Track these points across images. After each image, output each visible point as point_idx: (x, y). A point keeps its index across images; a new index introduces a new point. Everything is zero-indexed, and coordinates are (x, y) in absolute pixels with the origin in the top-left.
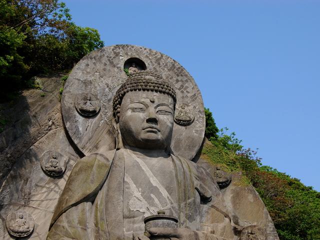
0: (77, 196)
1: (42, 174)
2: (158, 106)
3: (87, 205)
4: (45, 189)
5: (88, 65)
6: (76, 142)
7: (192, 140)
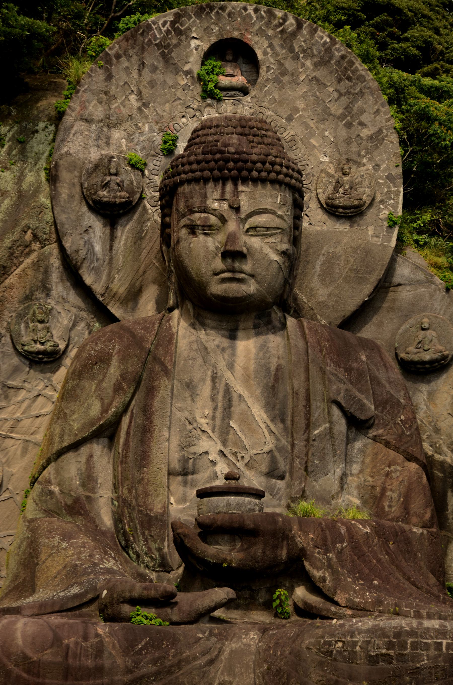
0: (77, 424)
1: (16, 360)
3: (97, 449)
4: (22, 394)
5: (109, 77)
6: (88, 279)
7: (366, 252)
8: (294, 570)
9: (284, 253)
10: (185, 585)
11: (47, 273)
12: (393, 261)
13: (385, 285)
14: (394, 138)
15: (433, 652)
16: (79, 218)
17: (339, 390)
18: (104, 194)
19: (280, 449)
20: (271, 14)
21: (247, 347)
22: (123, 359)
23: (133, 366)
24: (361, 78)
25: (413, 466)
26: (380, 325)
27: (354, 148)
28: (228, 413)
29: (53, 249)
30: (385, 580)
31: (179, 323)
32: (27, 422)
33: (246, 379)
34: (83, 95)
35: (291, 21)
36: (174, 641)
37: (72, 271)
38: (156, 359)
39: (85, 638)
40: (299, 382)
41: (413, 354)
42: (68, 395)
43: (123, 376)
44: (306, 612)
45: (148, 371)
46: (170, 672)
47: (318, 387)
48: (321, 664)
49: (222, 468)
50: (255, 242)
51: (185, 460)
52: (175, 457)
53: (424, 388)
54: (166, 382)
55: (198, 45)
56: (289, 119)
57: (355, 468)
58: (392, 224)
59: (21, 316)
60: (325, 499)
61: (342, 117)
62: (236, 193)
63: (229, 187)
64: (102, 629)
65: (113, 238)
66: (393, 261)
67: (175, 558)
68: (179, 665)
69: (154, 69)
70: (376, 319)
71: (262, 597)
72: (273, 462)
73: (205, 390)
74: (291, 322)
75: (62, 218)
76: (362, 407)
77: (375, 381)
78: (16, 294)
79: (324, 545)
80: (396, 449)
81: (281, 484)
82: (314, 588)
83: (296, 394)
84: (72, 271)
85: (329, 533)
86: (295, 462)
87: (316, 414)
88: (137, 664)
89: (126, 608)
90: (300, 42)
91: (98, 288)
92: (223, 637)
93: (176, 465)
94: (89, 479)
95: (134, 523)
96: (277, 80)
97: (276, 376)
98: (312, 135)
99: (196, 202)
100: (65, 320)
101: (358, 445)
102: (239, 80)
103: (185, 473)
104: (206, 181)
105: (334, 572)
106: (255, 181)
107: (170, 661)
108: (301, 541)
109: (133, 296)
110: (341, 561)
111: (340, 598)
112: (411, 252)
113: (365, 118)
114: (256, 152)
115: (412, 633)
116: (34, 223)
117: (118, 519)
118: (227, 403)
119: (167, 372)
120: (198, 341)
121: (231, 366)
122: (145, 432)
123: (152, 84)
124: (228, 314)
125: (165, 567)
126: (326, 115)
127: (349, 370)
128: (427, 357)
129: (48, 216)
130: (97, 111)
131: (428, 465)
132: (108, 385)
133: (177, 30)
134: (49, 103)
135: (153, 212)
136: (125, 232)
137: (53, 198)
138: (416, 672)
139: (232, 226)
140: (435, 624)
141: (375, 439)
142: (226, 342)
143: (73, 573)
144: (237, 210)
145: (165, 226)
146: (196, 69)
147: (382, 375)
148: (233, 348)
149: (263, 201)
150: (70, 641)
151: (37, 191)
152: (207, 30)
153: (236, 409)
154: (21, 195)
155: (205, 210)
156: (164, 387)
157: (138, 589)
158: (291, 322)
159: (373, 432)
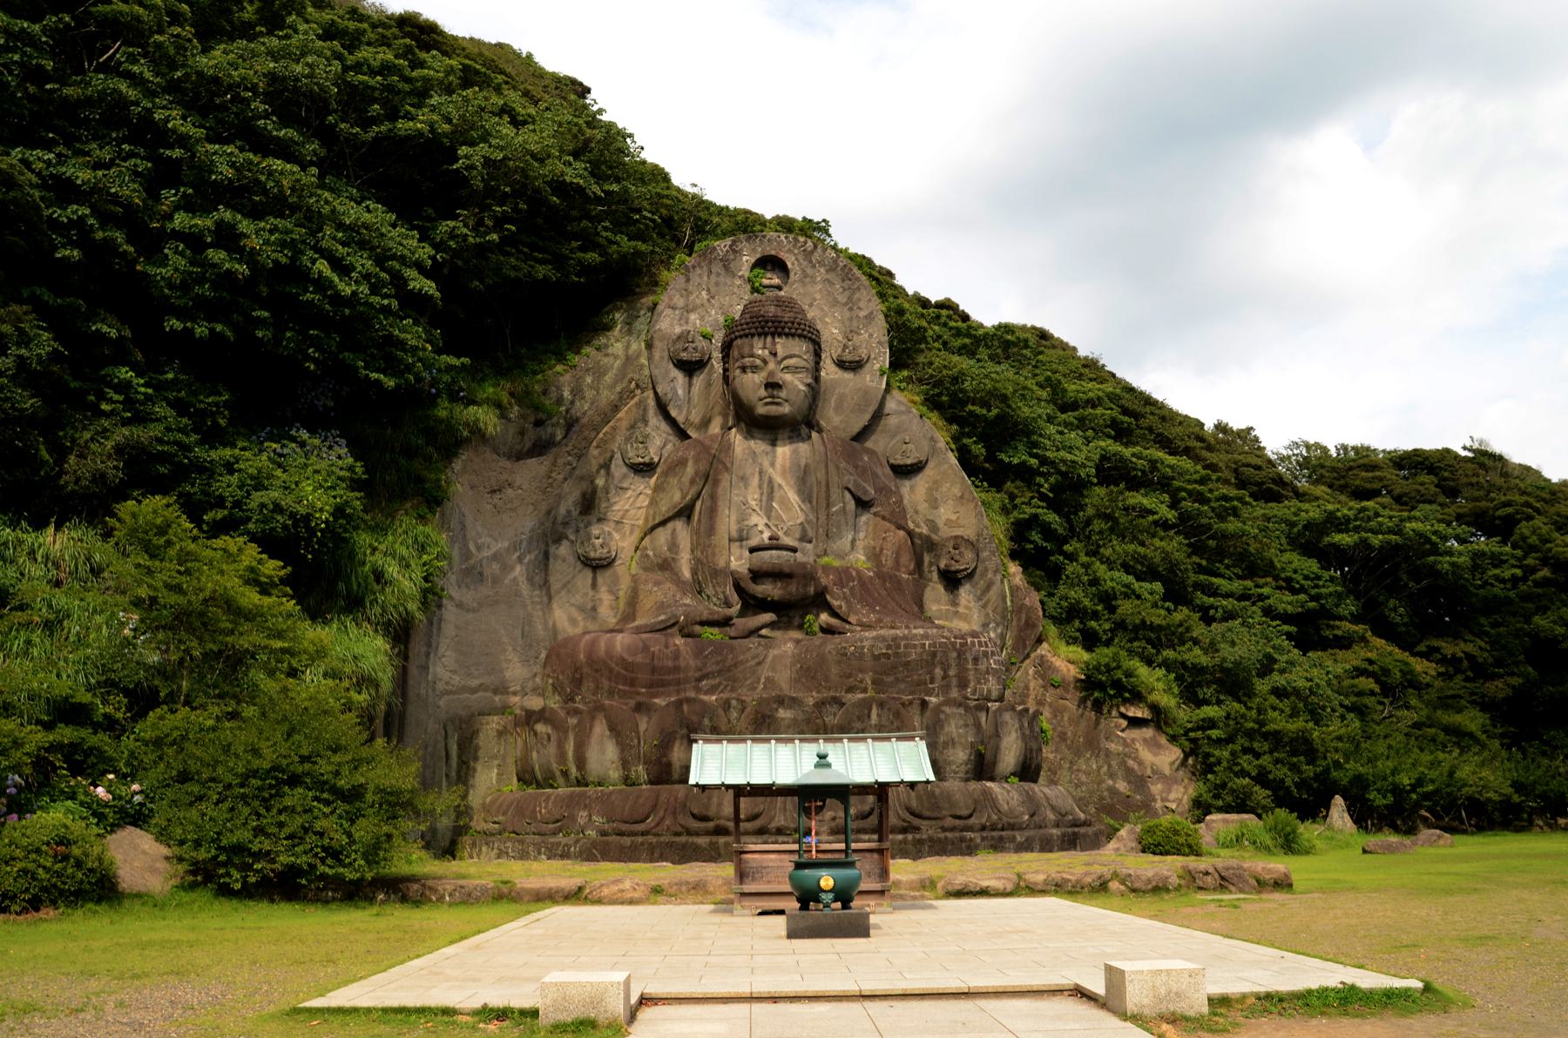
0: (665, 508)
1: (625, 469)
2: (785, 358)
3: (679, 525)
4: (630, 493)
5: (688, 280)
6: (673, 413)
7: (866, 393)
8: (819, 602)
9: (808, 385)
10: (742, 614)
11: (645, 410)
12: (883, 399)
13: (878, 415)
14: (882, 317)
15: (919, 650)
16: (667, 372)
17: (850, 480)
18: (684, 356)
19: (808, 522)
20: (796, 240)
21: (784, 451)
22: (696, 461)
23: (703, 466)
24: (858, 279)
25: (902, 533)
26: (876, 442)
27: (855, 324)
28: (771, 497)
29: (650, 394)
30: (884, 607)
31: (737, 438)
32: (633, 512)
33: (784, 474)
34: (670, 291)
35: (810, 243)
36: (732, 649)
37: (662, 408)
38: (720, 461)
39: (667, 647)
40: (821, 475)
41: (899, 460)
42: (658, 489)
43: (696, 473)
44: (828, 630)
45: (713, 468)
46: (729, 670)
47: (834, 478)
48: (839, 663)
49: (766, 535)
50: (788, 377)
51: (740, 531)
52: (734, 528)
53: (907, 483)
54: (727, 476)
55: (748, 259)
56: (811, 305)
57: (862, 535)
59: (628, 439)
60: (841, 556)
61: (846, 304)
62: (774, 344)
63: (769, 339)
64: (679, 641)
65: (690, 385)
66: (883, 399)
67: (735, 598)
68: (736, 665)
69: (718, 275)
70: (873, 438)
71: (796, 621)
72: (804, 531)
73: (755, 481)
74: (814, 434)
75: (656, 372)
76: (866, 492)
77: (875, 475)
78: (625, 424)
79: (841, 583)
80: (890, 521)
81: (809, 546)
82: (834, 614)
83: (819, 483)
84: (662, 408)
85: (844, 575)
86: (821, 529)
87: (834, 497)
88: (705, 665)
89: (697, 628)
90: (816, 256)
91: (680, 419)
92: (767, 647)
93: (734, 534)
94: (673, 546)
95: (706, 573)
96: (801, 281)
97: (805, 472)
98: (826, 315)
99: (746, 351)
100: (658, 442)
101: (864, 518)
102: (776, 281)
103: (741, 540)
104: (753, 335)
105: (848, 602)
106: (787, 335)
107: (729, 662)
108: (824, 581)
109: (705, 423)
110: (852, 594)
111: (852, 619)
112: (895, 392)
113: (861, 304)
114: (787, 316)
115: (905, 638)
116: (636, 376)
117: (694, 573)
118: (770, 490)
119: (727, 469)
120: (749, 448)
121: (772, 464)
122: (712, 511)
123: (717, 284)
124: (769, 428)
125: (728, 605)
126: (835, 303)
127: (856, 467)
128: (909, 462)
129: (646, 372)
130: (680, 302)
131: (910, 534)
132: (686, 479)
133: (734, 250)
134: (648, 300)
135: (717, 366)
136: (699, 381)
137: (650, 359)
138: (907, 664)
139: (771, 366)
140: (921, 631)
141: (875, 514)
142: (769, 448)
143: (661, 607)
144: (775, 355)
145: (725, 370)
146: (747, 274)
147: (879, 471)
148: (774, 452)
149: (793, 349)
150: (655, 649)
151: (639, 356)
152: (754, 250)
153: (777, 494)
154: (628, 358)
155: (752, 356)
156: (725, 479)
157: (706, 616)
158: (814, 434)
159: (873, 510)
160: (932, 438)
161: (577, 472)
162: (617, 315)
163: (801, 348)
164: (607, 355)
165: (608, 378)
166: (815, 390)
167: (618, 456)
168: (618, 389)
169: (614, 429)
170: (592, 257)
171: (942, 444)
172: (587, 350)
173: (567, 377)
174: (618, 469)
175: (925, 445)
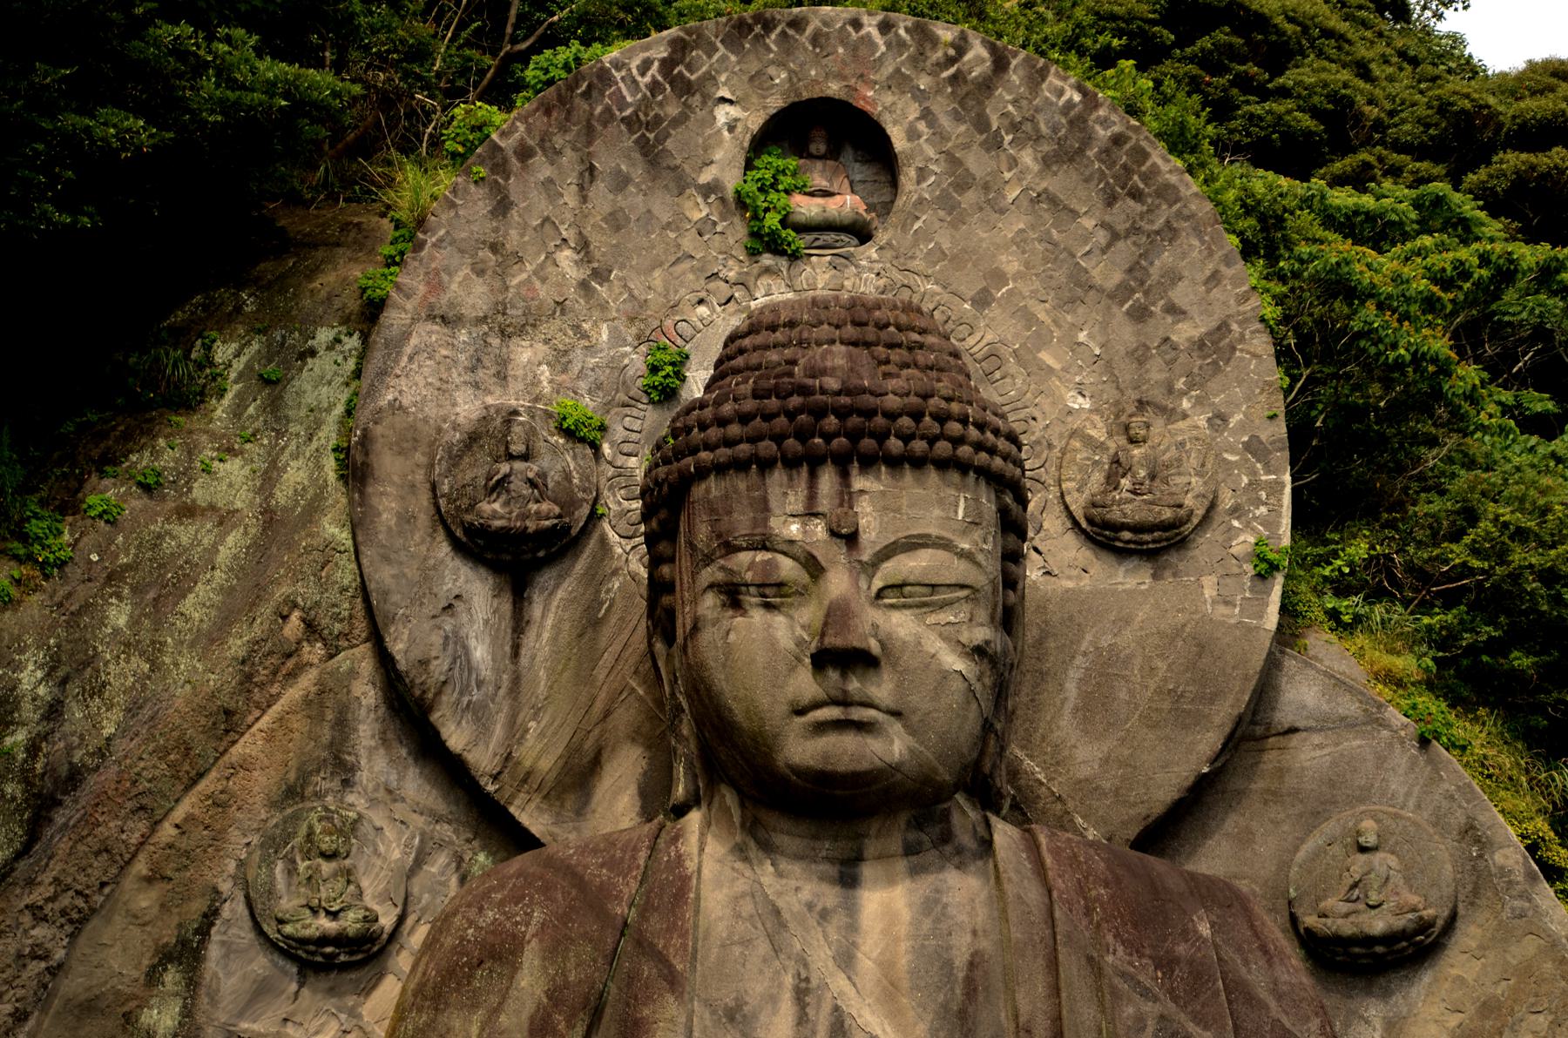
1: (261, 963)
5: (502, 207)
6: (456, 737)
7: (1201, 646)
9: (979, 652)
11: (343, 725)
12: (1272, 666)
13: (1253, 732)
14: (1262, 345)
16: (428, 575)
18: (494, 510)
20: (924, 37)
21: (887, 903)
22: (555, 948)
23: (580, 967)
24: (1167, 193)
26: (1245, 839)
27: (1156, 372)
29: (361, 659)
31: (705, 848)
33: (889, 993)
34: (434, 254)
37: (410, 714)
38: (643, 946)
40: (1031, 999)
43: (555, 996)
50: (902, 624)
53: (1374, 1010)
54: (670, 1007)
55: (733, 118)
56: (982, 300)
58: (1266, 570)
59: (274, 844)
61: (1121, 293)
62: (847, 497)
63: (827, 480)
65: (519, 624)
66: (1272, 666)
69: (621, 182)
70: (1232, 823)
74: (1004, 834)
75: (382, 576)
77: (1238, 991)
78: (262, 783)
84: (410, 714)
90: (1003, 103)
91: (482, 760)
96: (946, 202)
97: (969, 982)
98: (1042, 341)
99: (742, 522)
100: (394, 849)
102: (847, 204)
104: (766, 465)
106: (895, 463)
109: (577, 779)
112: (1321, 642)
113: (1181, 294)
114: (896, 390)
116: (306, 592)
119: (673, 981)
120: (756, 892)
121: (846, 960)
123: (616, 221)
126: (1078, 288)
127: (1166, 964)
128: (1378, 924)
129: (345, 574)
130: (473, 295)
133: (677, 78)
135: (627, 555)
136: (554, 605)
137: (356, 526)
139: (838, 582)
142: (830, 896)
144: (851, 539)
145: (659, 588)
146: (732, 180)
147: (1256, 976)
148: (852, 910)
151: (314, 509)
152: (758, 80)
154: (270, 519)
155: (764, 543)
158: (1004, 834)
160: (1470, 832)
161: (73, 985)
162: (223, 352)
163: (945, 509)
164: (188, 512)
165: (197, 606)
166: (1003, 673)
167: (234, 909)
168: (236, 646)
169: (219, 803)
170: (122, 127)
171: (1510, 856)
172: (105, 493)
173: (34, 607)
174: (234, 962)
175: (1444, 858)
